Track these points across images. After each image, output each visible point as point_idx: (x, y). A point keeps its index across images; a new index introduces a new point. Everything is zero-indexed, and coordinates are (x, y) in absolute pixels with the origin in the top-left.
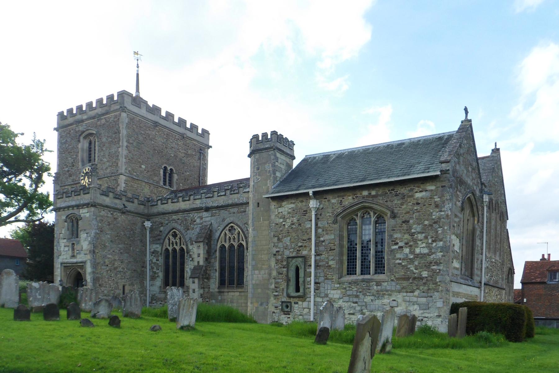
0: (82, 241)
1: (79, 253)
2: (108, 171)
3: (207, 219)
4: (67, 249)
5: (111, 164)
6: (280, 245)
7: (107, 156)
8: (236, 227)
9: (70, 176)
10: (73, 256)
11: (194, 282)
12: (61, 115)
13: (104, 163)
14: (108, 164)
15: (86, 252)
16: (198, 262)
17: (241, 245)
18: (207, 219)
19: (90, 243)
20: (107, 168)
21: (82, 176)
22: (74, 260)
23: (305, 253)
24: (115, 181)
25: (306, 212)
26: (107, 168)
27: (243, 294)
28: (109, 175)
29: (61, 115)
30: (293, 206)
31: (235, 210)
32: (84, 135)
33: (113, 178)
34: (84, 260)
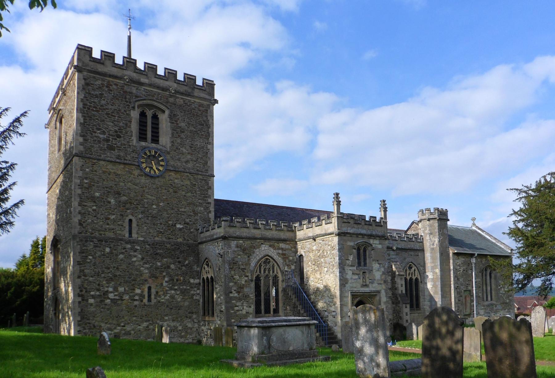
0: (374, 271)
1: (372, 283)
2: (190, 165)
3: (394, 257)
4: (356, 277)
5: (194, 159)
6: (459, 282)
7: (188, 147)
8: (413, 265)
9: (111, 148)
10: (366, 286)
11: (406, 307)
12: (84, 51)
13: (183, 154)
14: (189, 157)
15: (380, 282)
16: (402, 291)
17: (417, 279)
18: (394, 257)
19: (384, 273)
20: (187, 162)
21: (143, 158)
22: (366, 290)
23: (470, 288)
24: (203, 182)
25: (470, 264)
26: (187, 162)
27: (420, 314)
28: (192, 171)
29: (84, 51)
30: (464, 259)
31: (412, 253)
32: (141, 102)
33: (201, 177)
34: (378, 289)
